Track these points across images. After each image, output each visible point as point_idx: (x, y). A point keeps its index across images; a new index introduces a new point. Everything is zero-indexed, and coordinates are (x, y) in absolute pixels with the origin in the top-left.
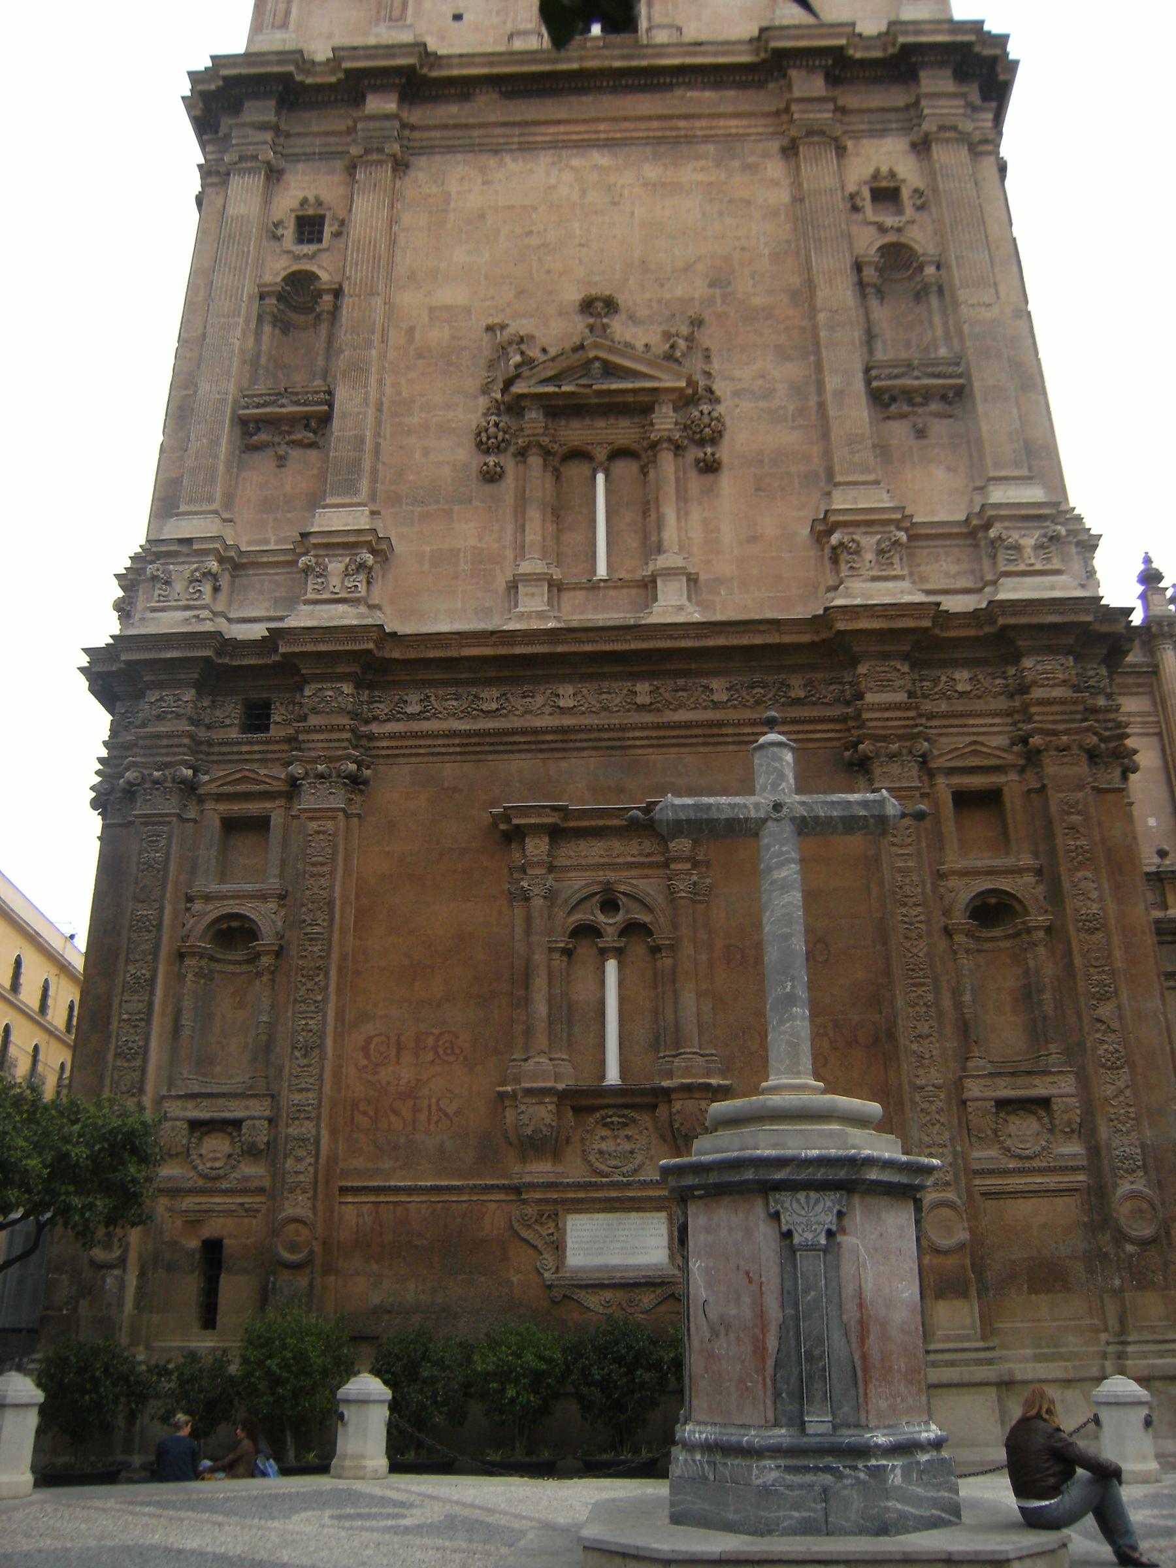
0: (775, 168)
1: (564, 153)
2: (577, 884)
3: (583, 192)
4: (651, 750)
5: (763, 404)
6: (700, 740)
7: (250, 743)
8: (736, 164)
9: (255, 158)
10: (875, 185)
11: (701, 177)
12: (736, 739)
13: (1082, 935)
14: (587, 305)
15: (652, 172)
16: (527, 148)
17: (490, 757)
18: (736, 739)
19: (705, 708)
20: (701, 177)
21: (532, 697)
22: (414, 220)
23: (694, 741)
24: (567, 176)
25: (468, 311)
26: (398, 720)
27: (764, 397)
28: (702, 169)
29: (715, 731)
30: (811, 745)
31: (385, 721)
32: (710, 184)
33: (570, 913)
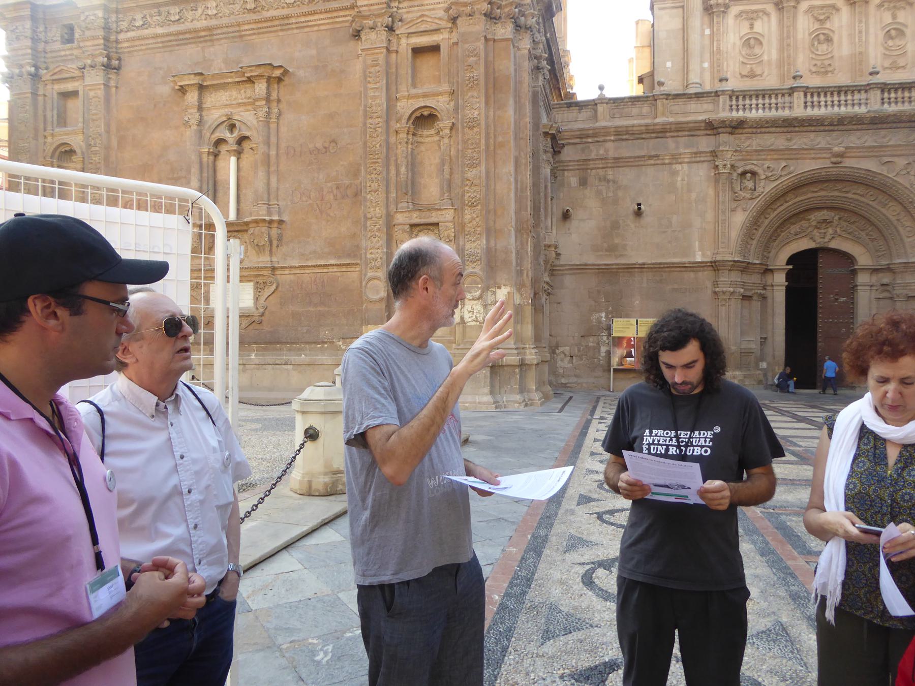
2: (214, 116)
4: (254, 37)
6: (279, 28)
7: (64, 50)
12: (297, 25)
13: (466, 130)
17: (177, 48)
18: (297, 25)
19: (283, 8)
21: (196, 10)
23: (275, 29)
26: (133, 30)
29: (286, 21)
30: (338, 26)
31: (126, 32)
33: (212, 133)
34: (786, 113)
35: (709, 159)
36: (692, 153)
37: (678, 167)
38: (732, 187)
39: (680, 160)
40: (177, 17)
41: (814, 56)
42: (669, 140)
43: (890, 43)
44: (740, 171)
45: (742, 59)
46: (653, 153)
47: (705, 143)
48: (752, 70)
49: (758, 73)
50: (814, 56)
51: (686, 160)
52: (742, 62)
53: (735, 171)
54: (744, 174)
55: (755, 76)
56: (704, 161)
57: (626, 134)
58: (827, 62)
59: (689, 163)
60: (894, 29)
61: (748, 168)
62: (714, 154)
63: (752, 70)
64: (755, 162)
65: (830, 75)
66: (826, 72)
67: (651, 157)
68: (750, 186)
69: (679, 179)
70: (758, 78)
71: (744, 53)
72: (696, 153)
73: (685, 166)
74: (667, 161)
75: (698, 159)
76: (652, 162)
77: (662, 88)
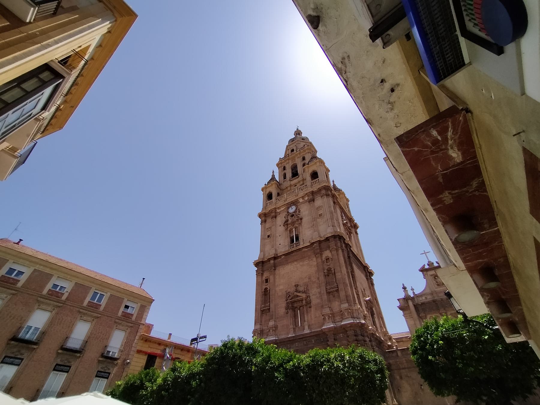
0: (315, 259)
1: (291, 263)
3: (294, 268)
5: (315, 296)
8: (310, 259)
9: (260, 273)
10: (326, 258)
11: (307, 263)
14: (295, 286)
15: (301, 263)
16: (288, 263)
20: (307, 263)
22: (277, 277)
24: (292, 266)
25: (283, 289)
27: (316, 295)
28: (307, 261)
32: (308, 263)
40: (289, 347)
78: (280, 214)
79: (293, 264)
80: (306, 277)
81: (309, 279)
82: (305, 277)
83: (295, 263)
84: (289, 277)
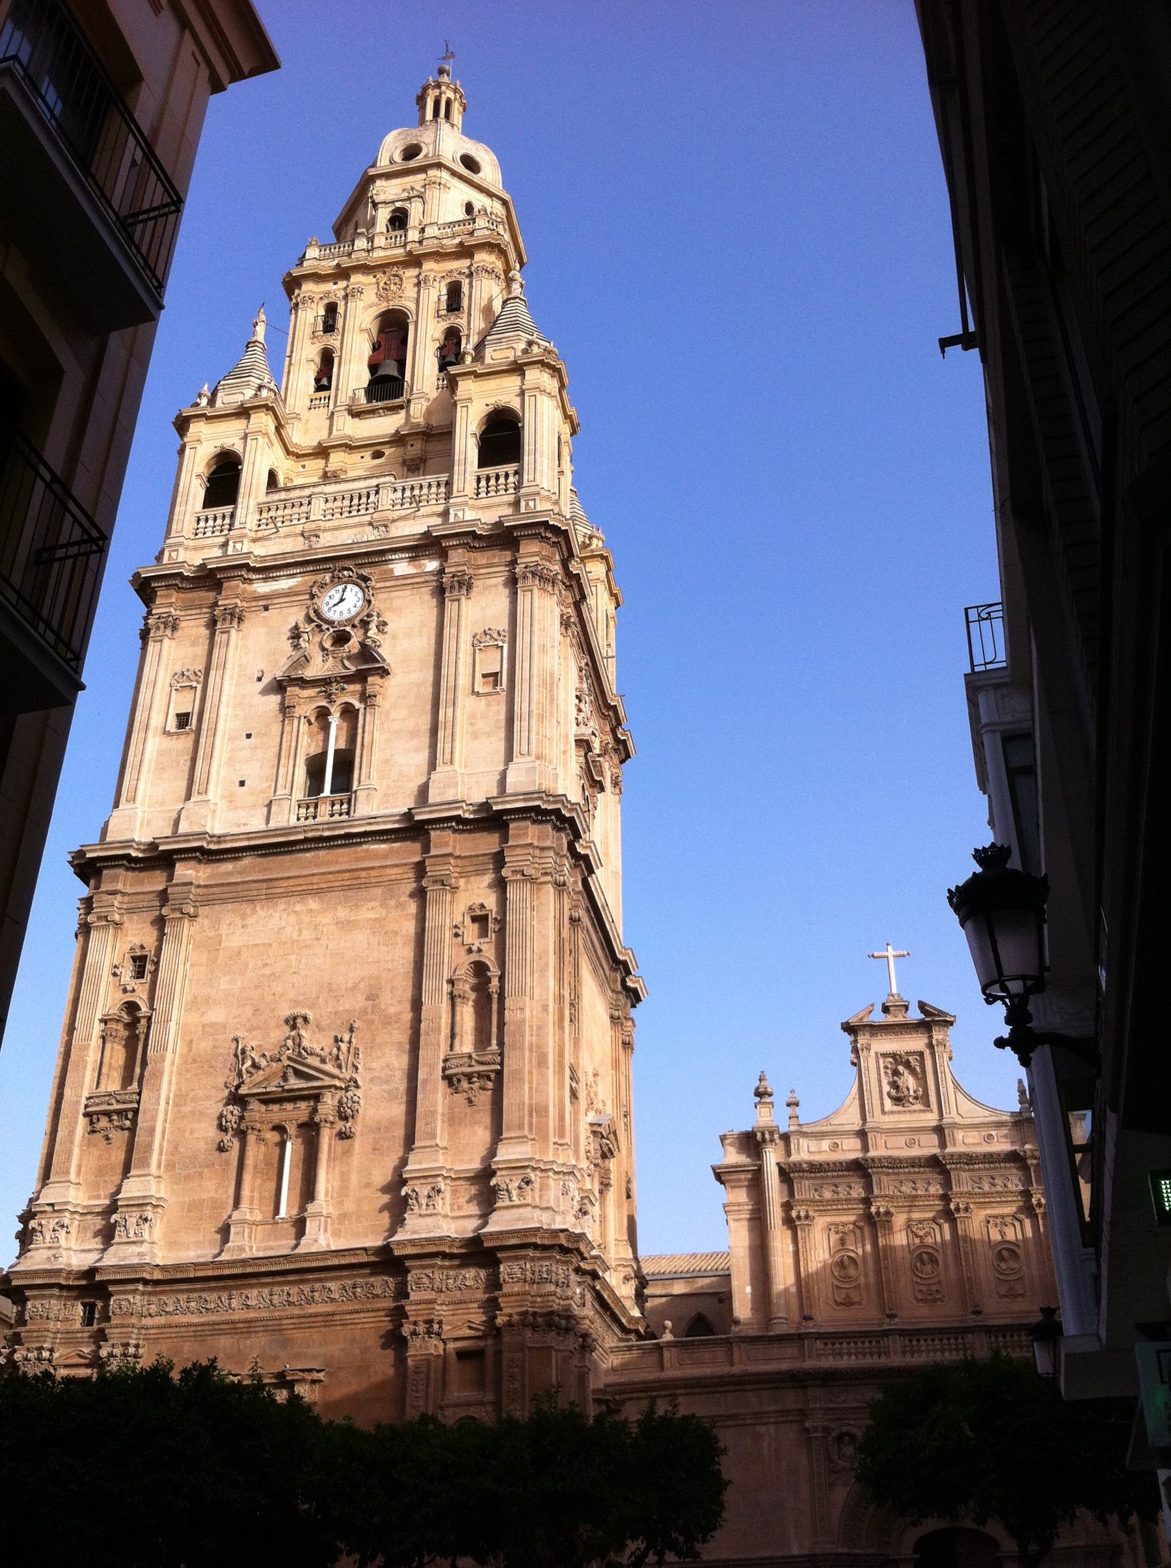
3: (300, 930)
34: (883, 1361)
35: (799, 1418)
36: (776, 1412)
37: (762, 1429)
38: (828, 1455)
39: (764, 1421)
41: (919, 1281)
42: (751, 1394)
43: (1003, 1266)
44: (834, 1434)
45: (835, 1282)
46: (733, 1411)
47: (791, 1400)
48: (848, 1296)
49: (855, 1300)
50: (919, 1281)
51: (771, 1420)
52: (837, 1286)
53: (830, 1433)
54: (840, 1438)
55: (853, 1304)
56: (791, 1422)
57: (699, 1387)
58: (934, 1288)
59: (774, 1423)
60: (1004, 1249)
61: (844, 1429)
62: (803, 1414)
63: (848, 1296)
64: (852, 1422)
65: (939, 1303)
66: (935, 1300)
67: (730, 1417)
68: (849, 1453)
69: (765, 1444)
70: (856, 1306)
71: (836, 1274)
72: (782, 1411)
73: (772, 1427)
74: (749, 1422)
75: (785, 1419)
76: (731, 1423)
77: (738, 1328)
78: (266, 608)
79: (298, 908)
80: (355, 988)
81: (368, 999)
82: (350, 985)
83: (313, 903)
84: (267, 971)
